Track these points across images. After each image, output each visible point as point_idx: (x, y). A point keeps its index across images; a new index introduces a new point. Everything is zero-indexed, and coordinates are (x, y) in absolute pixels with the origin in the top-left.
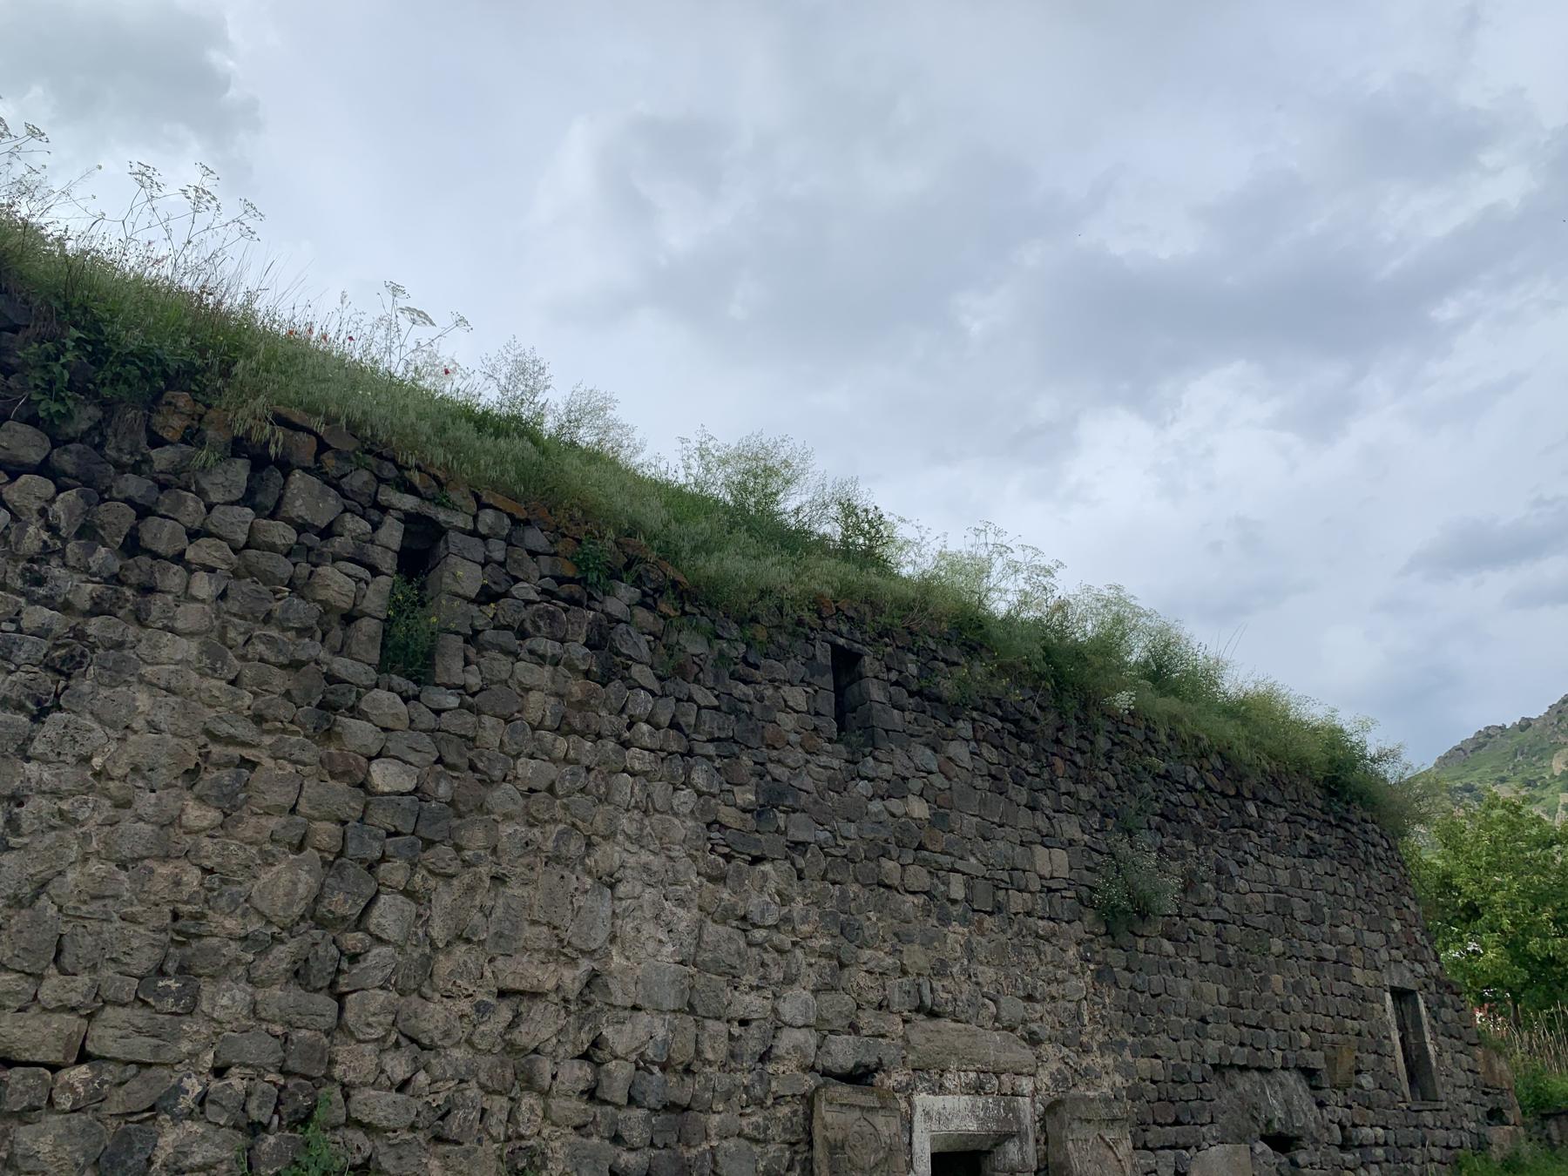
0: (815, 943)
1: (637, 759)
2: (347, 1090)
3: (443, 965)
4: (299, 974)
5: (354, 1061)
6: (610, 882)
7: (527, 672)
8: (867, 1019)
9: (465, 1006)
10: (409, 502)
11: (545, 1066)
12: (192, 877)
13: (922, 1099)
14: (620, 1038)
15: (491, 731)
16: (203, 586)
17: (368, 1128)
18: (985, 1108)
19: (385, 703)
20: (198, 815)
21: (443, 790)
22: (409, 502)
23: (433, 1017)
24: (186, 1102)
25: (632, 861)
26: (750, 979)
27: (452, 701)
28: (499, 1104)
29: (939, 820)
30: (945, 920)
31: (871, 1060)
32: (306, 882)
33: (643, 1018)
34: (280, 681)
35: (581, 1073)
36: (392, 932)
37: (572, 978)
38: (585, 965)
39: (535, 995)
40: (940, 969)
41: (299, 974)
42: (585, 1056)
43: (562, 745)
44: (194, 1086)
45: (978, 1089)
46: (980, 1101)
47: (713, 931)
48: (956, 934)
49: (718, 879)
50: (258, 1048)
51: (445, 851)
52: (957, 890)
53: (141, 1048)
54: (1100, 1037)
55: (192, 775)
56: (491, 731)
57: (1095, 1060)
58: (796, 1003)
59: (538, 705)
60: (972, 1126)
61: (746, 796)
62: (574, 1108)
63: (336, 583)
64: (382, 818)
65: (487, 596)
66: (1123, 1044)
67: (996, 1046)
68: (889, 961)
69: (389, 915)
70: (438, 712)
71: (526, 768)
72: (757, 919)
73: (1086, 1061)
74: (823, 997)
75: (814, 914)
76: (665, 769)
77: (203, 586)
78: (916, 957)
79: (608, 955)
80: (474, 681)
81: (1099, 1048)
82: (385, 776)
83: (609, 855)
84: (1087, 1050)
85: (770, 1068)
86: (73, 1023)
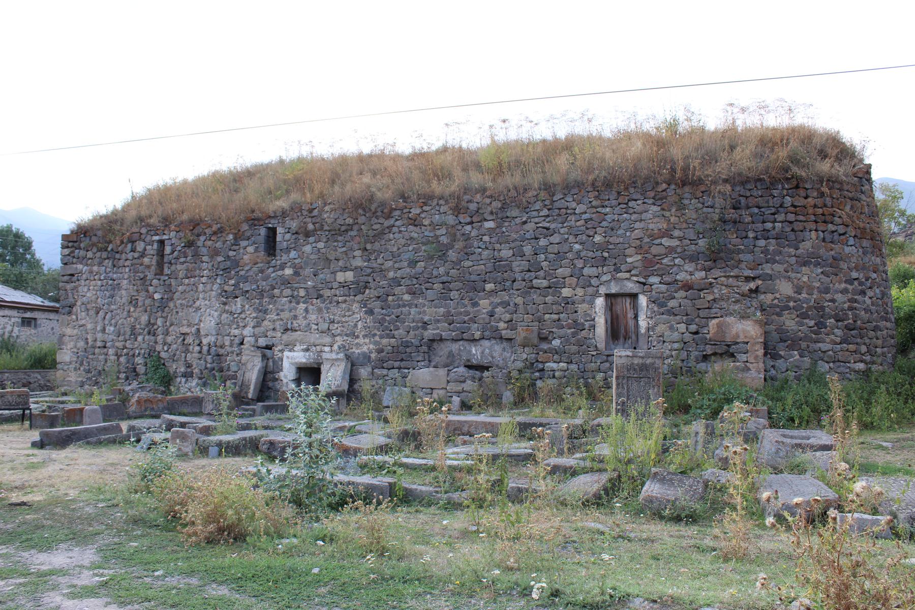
0: (251, 316)
1: (204, 280)
2: (159, 352)
3: (171, 329)
4: (149, 333)
5: (159, 348)
6: (198, 309)
7: (179, 267)
8: (270, 334)
9: (174, 337)
10: (156, 238)
11: (191, 347)
12: (132, 320)
13: (286, 353)
14: (205, 341)
15: (173, 282)
16: (127, 270)
17: (164, 359)
18: (309, 356)
19: (155, 282)
20: (132, 309)
21: (166, 297)
22: (156, 238)
23: (169, 339)
24: (136, 354)
25: (202, 303)
26: (235, 326)
27: (167, 278)
28: (183, 355)
29: (296, 274)
30: (298, 303)
31: (271, 343)
32: (147, 318)
33: (210, 337)
34: (139, 282)
35: (197, 348)
36: (160, 325)
37: (193, 330)
38: (196, 327)
39: (188, 334)
40: (295, 317)
41: (149, 333)
42: (199, 345)
43: (187, 281)
44: (137, 352)
45: (307, 350)
46: (307, 354)
47: (225, 316)
48: (302, 306)
49: (225, 304)
50: (145, 346)
51: (167, 308)
52: (302, 293)
53: (131, 346)
54: (363, 333)
55: (131, 302)
56: (173, 282)
57: (361, 340)
58: (247, 331)
59: (181, 275)
60: (304, 360)
61: (232, 282)
62: (197, 355)
63: (146, 260)
64: (157, 304)
65: (173, 252)
66: (375, 335)
67: (314, 337)
68: (276, 317)
69: (160, 322)
70: (164, 281)
71: (180, 288)
72: (234, 312)
73: (357, 341)
74: (257, 329)
75: (251, 309)
76: (210, 281)
77: (127, 270)
78: (286, 315)
79: (200, 325)
80: (169, 272)
81: (363, 336)
82: (157, 296)
83: (198, 303)
84: (358, 337)
85: (242, 347)
86: (123, 343)
